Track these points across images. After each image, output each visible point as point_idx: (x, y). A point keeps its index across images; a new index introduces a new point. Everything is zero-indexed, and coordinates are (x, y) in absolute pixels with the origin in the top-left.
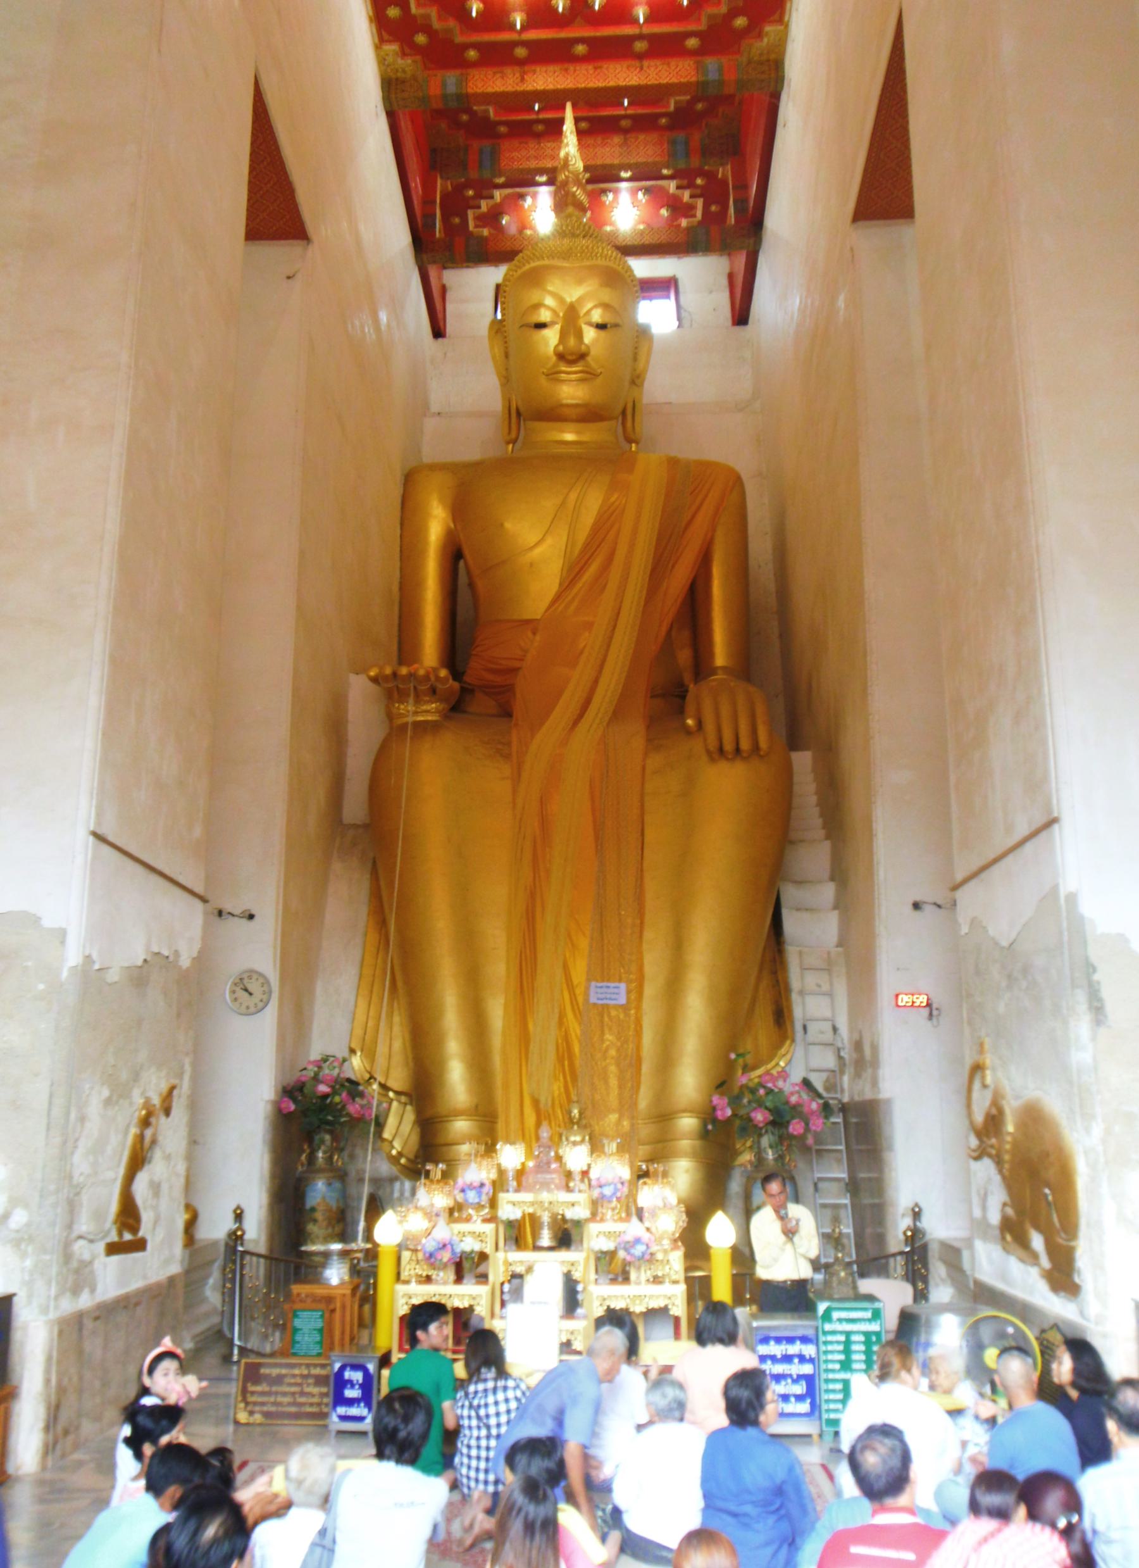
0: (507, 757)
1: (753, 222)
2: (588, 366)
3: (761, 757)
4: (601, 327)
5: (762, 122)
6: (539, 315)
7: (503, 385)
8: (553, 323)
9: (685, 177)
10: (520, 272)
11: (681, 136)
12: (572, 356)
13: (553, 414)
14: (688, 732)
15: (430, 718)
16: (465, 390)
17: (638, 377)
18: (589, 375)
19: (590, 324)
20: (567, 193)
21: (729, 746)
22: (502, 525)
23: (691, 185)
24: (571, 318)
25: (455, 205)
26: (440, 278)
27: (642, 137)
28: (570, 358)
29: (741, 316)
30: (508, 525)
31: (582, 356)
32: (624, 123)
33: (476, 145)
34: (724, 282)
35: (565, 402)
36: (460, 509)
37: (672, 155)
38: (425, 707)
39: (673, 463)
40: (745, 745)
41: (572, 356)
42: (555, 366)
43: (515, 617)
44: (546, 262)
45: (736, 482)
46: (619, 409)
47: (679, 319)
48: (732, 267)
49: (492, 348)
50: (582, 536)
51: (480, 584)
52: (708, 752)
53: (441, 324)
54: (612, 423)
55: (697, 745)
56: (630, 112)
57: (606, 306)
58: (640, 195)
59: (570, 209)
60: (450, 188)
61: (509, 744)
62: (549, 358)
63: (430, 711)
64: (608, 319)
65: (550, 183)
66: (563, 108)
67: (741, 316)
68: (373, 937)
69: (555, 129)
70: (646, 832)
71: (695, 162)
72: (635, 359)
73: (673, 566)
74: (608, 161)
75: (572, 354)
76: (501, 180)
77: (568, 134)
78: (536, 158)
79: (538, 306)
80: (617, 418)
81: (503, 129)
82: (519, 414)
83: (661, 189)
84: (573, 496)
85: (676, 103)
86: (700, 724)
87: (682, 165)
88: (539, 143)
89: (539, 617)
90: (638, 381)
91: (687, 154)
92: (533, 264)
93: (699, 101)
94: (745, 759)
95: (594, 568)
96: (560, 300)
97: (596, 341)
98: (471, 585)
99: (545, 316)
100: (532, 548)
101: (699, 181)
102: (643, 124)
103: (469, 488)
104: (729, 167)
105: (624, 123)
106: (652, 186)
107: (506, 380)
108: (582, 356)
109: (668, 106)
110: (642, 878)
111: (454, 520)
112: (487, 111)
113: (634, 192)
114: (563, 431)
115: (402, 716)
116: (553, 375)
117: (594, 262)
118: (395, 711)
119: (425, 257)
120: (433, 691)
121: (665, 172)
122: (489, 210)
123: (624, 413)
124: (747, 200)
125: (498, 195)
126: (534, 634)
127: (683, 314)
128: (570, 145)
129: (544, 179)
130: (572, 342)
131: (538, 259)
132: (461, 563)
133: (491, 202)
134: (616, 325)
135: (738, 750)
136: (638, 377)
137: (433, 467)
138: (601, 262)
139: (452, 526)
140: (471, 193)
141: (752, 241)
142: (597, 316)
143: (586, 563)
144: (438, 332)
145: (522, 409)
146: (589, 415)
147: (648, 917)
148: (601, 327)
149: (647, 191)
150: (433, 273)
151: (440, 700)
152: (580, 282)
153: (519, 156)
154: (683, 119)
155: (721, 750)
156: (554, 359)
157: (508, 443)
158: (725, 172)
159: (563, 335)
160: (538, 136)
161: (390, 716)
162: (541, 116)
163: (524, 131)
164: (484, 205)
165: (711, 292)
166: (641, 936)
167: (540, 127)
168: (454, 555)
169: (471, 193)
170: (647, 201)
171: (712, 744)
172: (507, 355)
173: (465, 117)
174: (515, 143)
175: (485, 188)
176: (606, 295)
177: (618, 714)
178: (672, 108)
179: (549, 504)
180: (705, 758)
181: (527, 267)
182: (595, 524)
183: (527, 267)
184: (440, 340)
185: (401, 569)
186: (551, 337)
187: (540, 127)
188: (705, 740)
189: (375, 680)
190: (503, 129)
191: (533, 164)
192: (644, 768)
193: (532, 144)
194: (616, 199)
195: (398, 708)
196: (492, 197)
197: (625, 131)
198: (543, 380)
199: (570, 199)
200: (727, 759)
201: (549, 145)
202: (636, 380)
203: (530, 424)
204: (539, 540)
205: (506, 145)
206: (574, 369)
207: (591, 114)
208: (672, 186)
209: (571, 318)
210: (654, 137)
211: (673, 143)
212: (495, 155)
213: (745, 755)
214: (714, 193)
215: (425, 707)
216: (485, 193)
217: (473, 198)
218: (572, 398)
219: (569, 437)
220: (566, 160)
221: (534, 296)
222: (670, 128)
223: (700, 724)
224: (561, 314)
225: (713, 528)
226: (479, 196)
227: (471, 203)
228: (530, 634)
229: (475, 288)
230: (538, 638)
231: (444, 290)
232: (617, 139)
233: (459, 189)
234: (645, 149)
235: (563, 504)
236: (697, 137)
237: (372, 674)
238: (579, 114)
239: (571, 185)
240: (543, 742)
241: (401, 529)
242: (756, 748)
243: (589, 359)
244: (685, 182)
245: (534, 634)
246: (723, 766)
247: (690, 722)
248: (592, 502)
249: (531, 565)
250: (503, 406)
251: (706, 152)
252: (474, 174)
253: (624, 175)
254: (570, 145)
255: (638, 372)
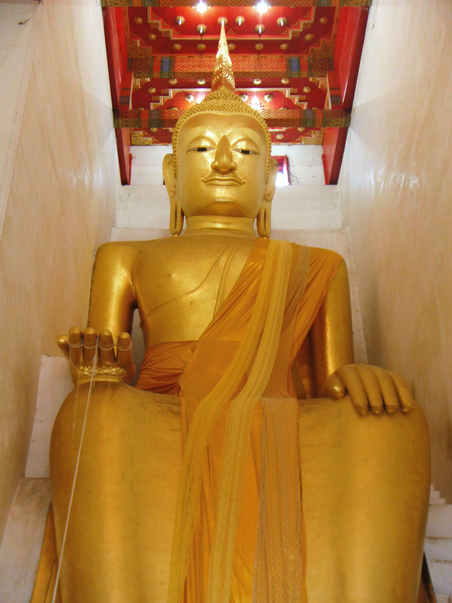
0: (178, 414)
1: (346, 108)
2: (235, 175)
3: (405, 413)
4: (245, 152)
5: (355, 34)
6: (200, 143)
7: (172, 197)
8: (211, 148)
9: (296, 84)
10: (188, 118)
11: (294, 58)
12: (224, 170)
13: (209, 209)
14: (333, 397)
15: (110, 380)
16: (144, 209)
17: (269, 195)
18: (236, 183)
19: (237, 150)
20: (221, 78)
21: (376, 403)
22: (170, 275)
23: (300, 93)
24: (224, 146)
25: (143, 97)
26: (129, 150)
27: (269, 57)
28: (223, 170)
29: (332, 179)
30: (174, 276)
31: (232, 170)
32: (259, 47)
33: (159, 57)
34: (320, 161)
35: (218, 200)
36: (136, 271)
37: (289, 68)
38: (106, 371)
39: (295, 247)
40: (391, 401)
41: (224, 170)
42: (211, 175)
43: (179, 340)
44: (207, 112)
45: (340, 262)
46: (256, 213)
47: (289, 181)
48: (324, 151)
49: (164, 174)
50: (230, 286)
51: (150, 320)
52: (357, 408)
53: (128, 176)
54: (250, 220)
55: (345, 405)
56: (262, 38)
57: (248, 140)
58: (266, 98)
59: (223, 88)
60: (140, 87)
61: (179, 405)
62: (207, 171)
63: (112, 373)
64: (251, 148)
65: (207, 86)
66: (219, 33)
67: (332, 179)
68: (43, 575)
69: (213, 47)
70: (306, 477)
71: (304, 74)
72: (267, 183)
73: (299, 311)
74: (247, 70)
75: (224, 167)
76: (175, 82)
77: (222, 44)
78: (199, 66)
79: (200, 138)
80: (255, 218)
81: (178, 47)
82: (183, 214)
83: (281, 95)
84: (223, 260)
85: (293, 33)
86: (346, 392)
87: (295, 76)
88: (202, 58)
89: (197, 339)
90: (268, 198)
91: (300, 67)
92: (197, 114)
93: (308, 34)
94: (390, 415)
95: (238, 308)
96: (218, 134)
97: (242, 161)
98: (143, 324)
99: (204, 144)
100: (191, 292)
101: (306, 90)
102: (271, 48)
103: (145, 257)
104: (327, 78)
105: (259, 47)
106: (274, 92)
107: (173, 194)
108: (232, 170)
109: (287, 35)
110: (302, 517)
111: (132, 280)
112: (168, 33)
113: (262, 95)
114: (215, 222)
115: (85, 376)
116: (210, 182)
117: (240, 113)
118: (79, 372)
119: (120, 120)
120: (115, 360)
121: (283, 81)
122: (165, 104)
123: (258, 217)
124: (340, 96)
125: (171, 92)
126: (193, 351)
127: (292, 178)
128: (223, 50)
129: (202, 83)
130: (225, 159)
131: (201, 110)
132: (136, 311)
133: (167, 98)
134: (255, 153)
135: (384, 406)
136: (269, 195)
137: (118, 244)
138: (246, 114)
139: (131, 283)
140: (153, 90)
141: (344, 120)
142: (243, 145)
143: (234, 302)
144: (125, 181)
145: (185, 211)
146: (235, 211)
147: (310, 555)
148: (245, 152)
149: (271, 94)
150: (125, 148)
151: (121, 366)
152: (230, 124)
153: (187, 64)
154: (297, 46)
155: (369, 407)
156: (211, 170)
157: (174, 234)
158: (324, 82)
159: (218, 156)
160: (201, 52)
161: (75, 378)
162: (204, 38)
163: (190, 48)
164: (162, 100)
165: (311, 166)
166: (304, 574)
167: (203, 46)
168: (131, 304)
169: (153, 90)
170: (270, 102)
171: (360, 401)
172: (176, 176)
173: (153, 37)
174: (185, 57)
175: (163, 85)
176: (249, 132)
177: (268, 392)
178: (290, 38)
179: (206, 264)
180: (354, 415)
181: (194, 115)
182: (241, 276)
183: (194, 115)
184: (126, 186)
185: (90, 312)
186: (209, 158)
187: (203, 46)
188: (352, 400)
189: (65, 348)
190: (178, 47)
191: (197, 70)
192: (298, 424)
193: (197, 58)
194: (250, 99)
195: (83, 370)
196: (167, 95)
197: (259, 52)
198: (203, 186)
199: (223, 81)
200: (374, 414)
201: (207, 59)
202: (268, 198)
203: (191, 219)
204: (197, 292)
205: (179, 57)
206: (225, 178)
207: (235, 38)
208: (287, 92)
209: (224, 146)
210: (276, 57)
211: (289, 61)
212: (172, 63)
213: (390, 411)
214: (316, 98)
215: (106, 371)
216: (163, 91)
217: (155, 94)
218: (223, 198)
219: (219, 226)
220: (221, 59)
221: (197, 131)
222: (288, 52)
223: (346, 392)
224: (217, 143)
225: (327, 287)
226: (158, 93)
227: (154, 98)
228: (189, 351)
229: (151, 159)
230: (195, 353)
231: (131, 157)
232: (252, 57)
233: (146, 86)
234: (272, 64)
235: (217, 263)
236: (305, 58)
237: (62, 341)
238: (231, 38)
239: (224, 73)
240: (209, 405)
241: (92, 284)
242: (401, 405)
243: (236, 172)
244: (296, 90)
245: (193, 351)
246: (371, 420)
247: (337, 388)
248: (238, 265)
249: (192, 303)
250: (171, 211)
251: (312, 68)
252: (156, 75)
253: (257, 82)
254: (223, 50)
255: (267, 193)
